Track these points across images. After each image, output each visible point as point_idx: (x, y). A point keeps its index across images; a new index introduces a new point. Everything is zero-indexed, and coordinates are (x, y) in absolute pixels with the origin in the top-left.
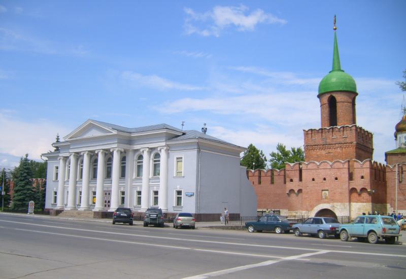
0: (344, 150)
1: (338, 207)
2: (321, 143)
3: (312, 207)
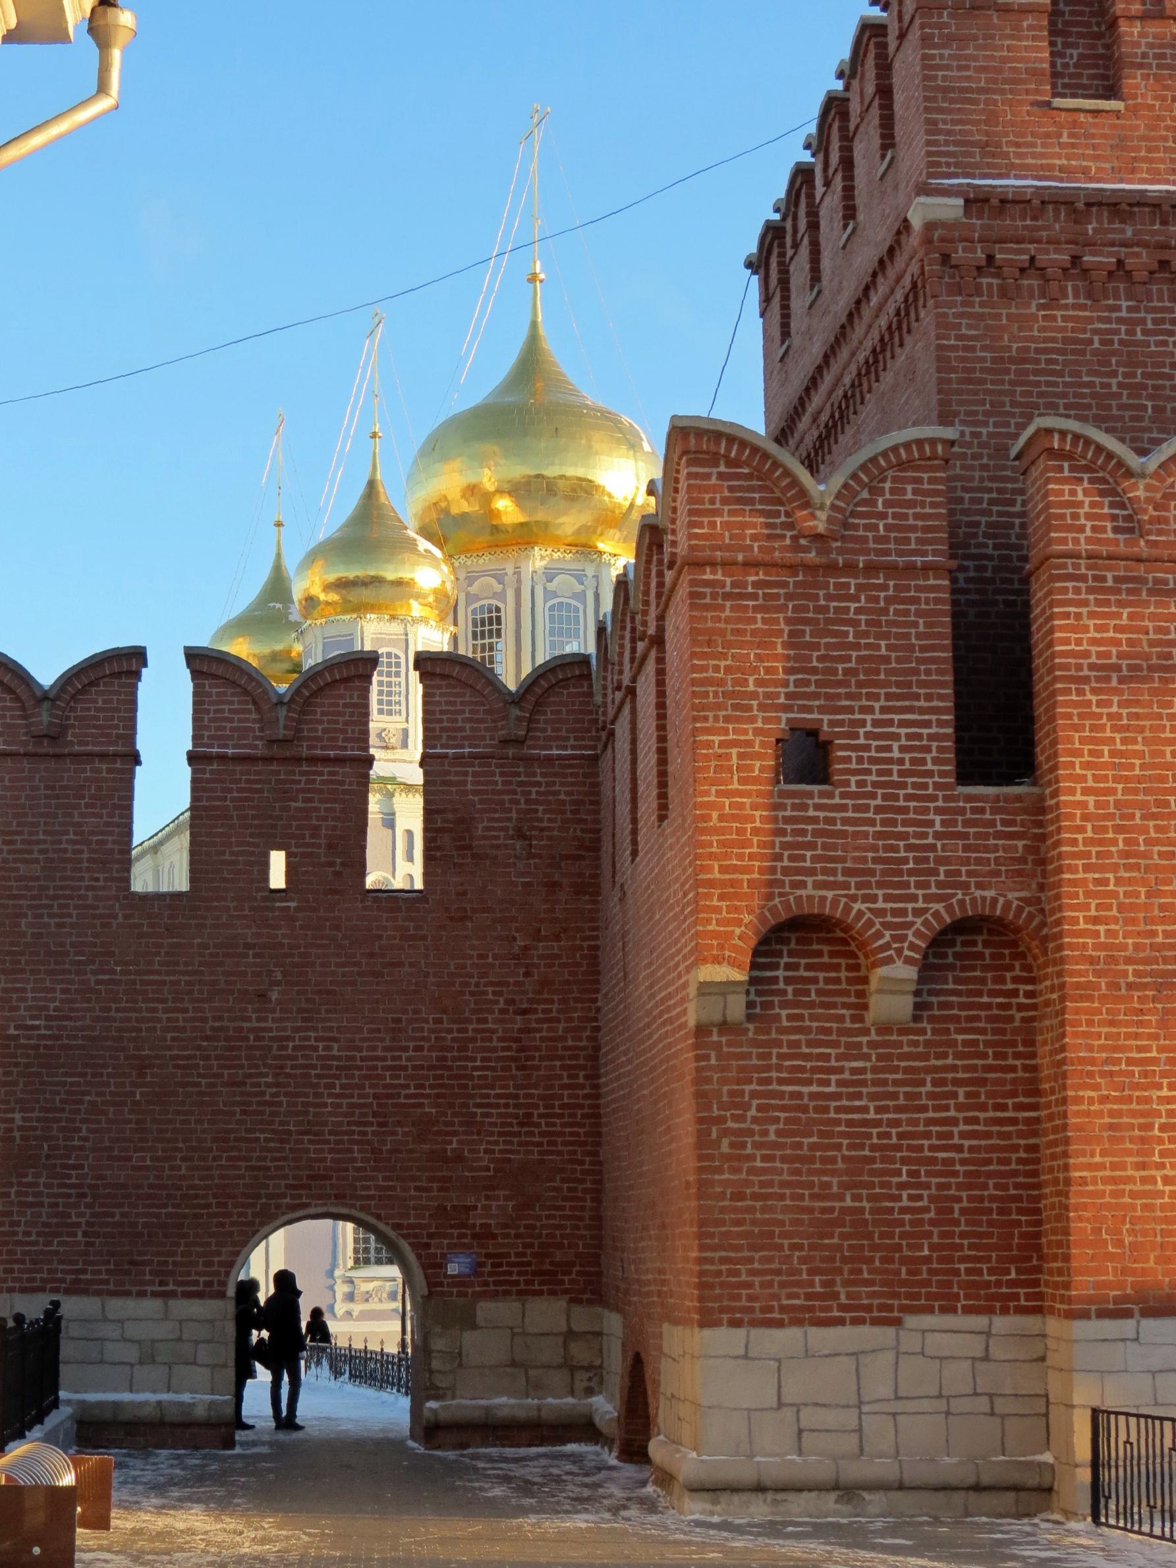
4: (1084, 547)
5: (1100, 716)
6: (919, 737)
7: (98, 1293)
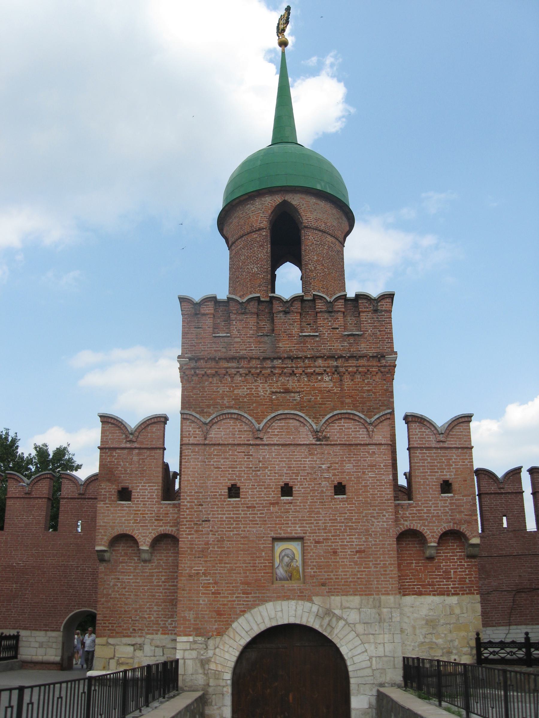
0: (347, 382)
1: (353, 616)
2: (255, 350)
3: (223, 619)
4: (191, 442)
5: (192, 483)
6: (152, 489)
7: (30, 630)
